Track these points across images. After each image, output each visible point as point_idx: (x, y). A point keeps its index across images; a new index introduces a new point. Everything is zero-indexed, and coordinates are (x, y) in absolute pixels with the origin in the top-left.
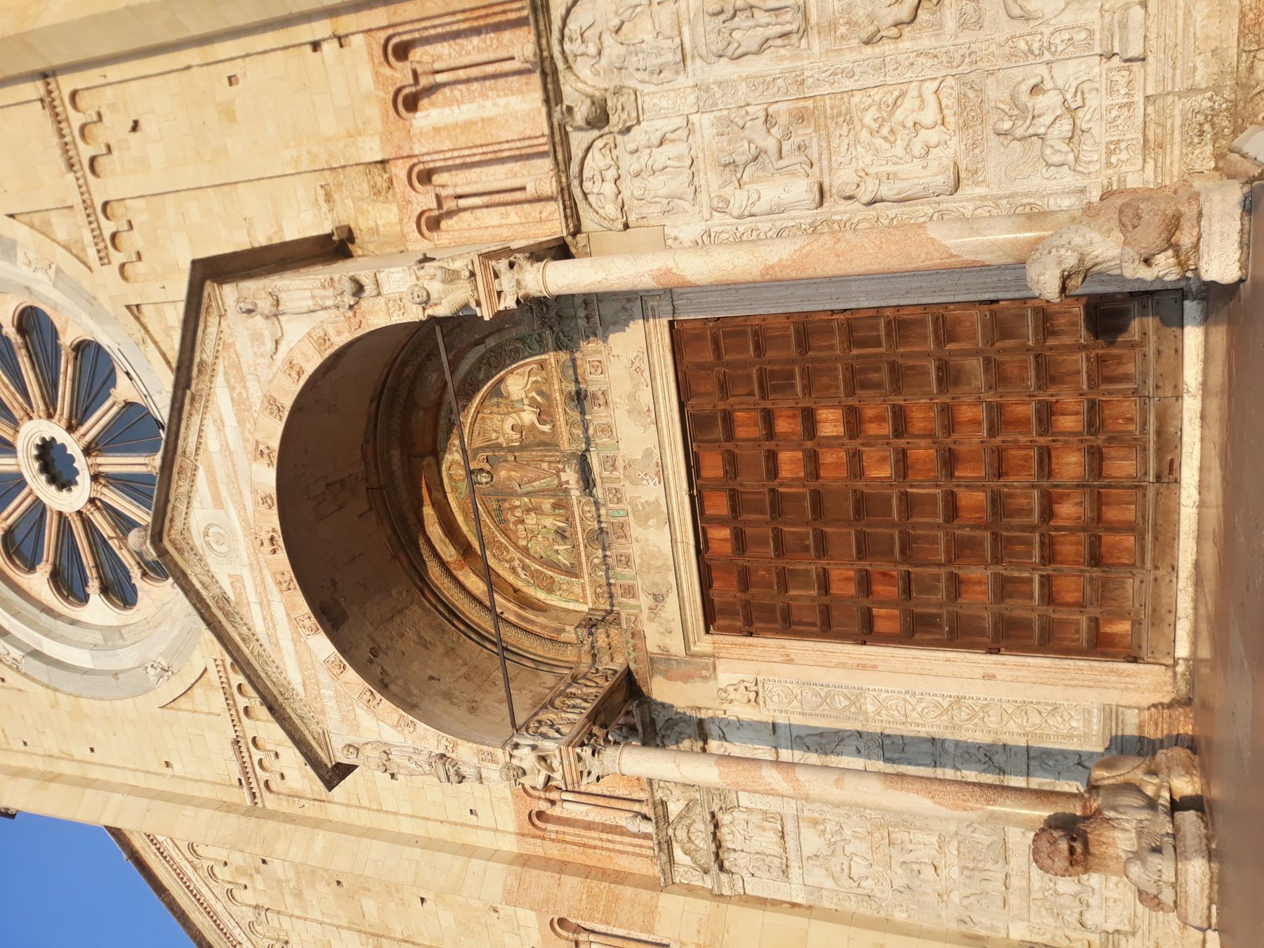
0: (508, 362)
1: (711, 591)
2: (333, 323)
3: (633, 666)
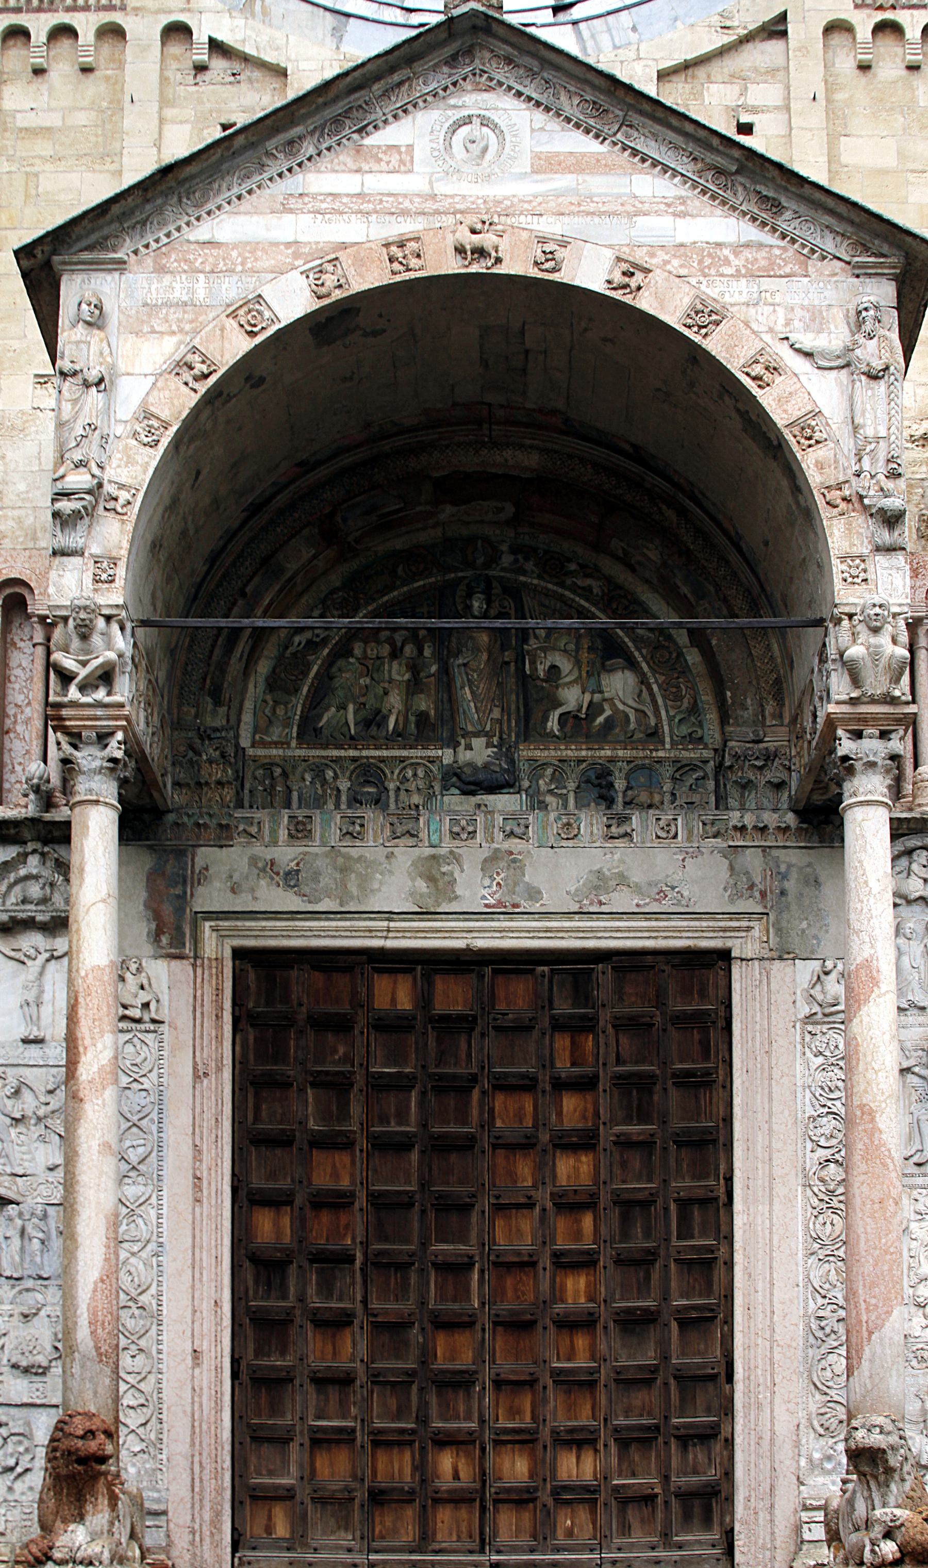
0: (661, 679)
1: (306, 967)
2: (836, 461)
3: (171, 817)
